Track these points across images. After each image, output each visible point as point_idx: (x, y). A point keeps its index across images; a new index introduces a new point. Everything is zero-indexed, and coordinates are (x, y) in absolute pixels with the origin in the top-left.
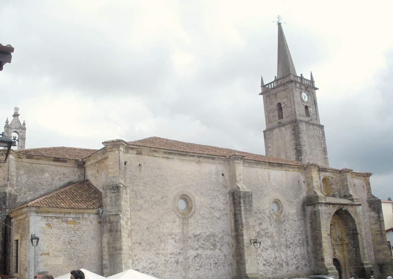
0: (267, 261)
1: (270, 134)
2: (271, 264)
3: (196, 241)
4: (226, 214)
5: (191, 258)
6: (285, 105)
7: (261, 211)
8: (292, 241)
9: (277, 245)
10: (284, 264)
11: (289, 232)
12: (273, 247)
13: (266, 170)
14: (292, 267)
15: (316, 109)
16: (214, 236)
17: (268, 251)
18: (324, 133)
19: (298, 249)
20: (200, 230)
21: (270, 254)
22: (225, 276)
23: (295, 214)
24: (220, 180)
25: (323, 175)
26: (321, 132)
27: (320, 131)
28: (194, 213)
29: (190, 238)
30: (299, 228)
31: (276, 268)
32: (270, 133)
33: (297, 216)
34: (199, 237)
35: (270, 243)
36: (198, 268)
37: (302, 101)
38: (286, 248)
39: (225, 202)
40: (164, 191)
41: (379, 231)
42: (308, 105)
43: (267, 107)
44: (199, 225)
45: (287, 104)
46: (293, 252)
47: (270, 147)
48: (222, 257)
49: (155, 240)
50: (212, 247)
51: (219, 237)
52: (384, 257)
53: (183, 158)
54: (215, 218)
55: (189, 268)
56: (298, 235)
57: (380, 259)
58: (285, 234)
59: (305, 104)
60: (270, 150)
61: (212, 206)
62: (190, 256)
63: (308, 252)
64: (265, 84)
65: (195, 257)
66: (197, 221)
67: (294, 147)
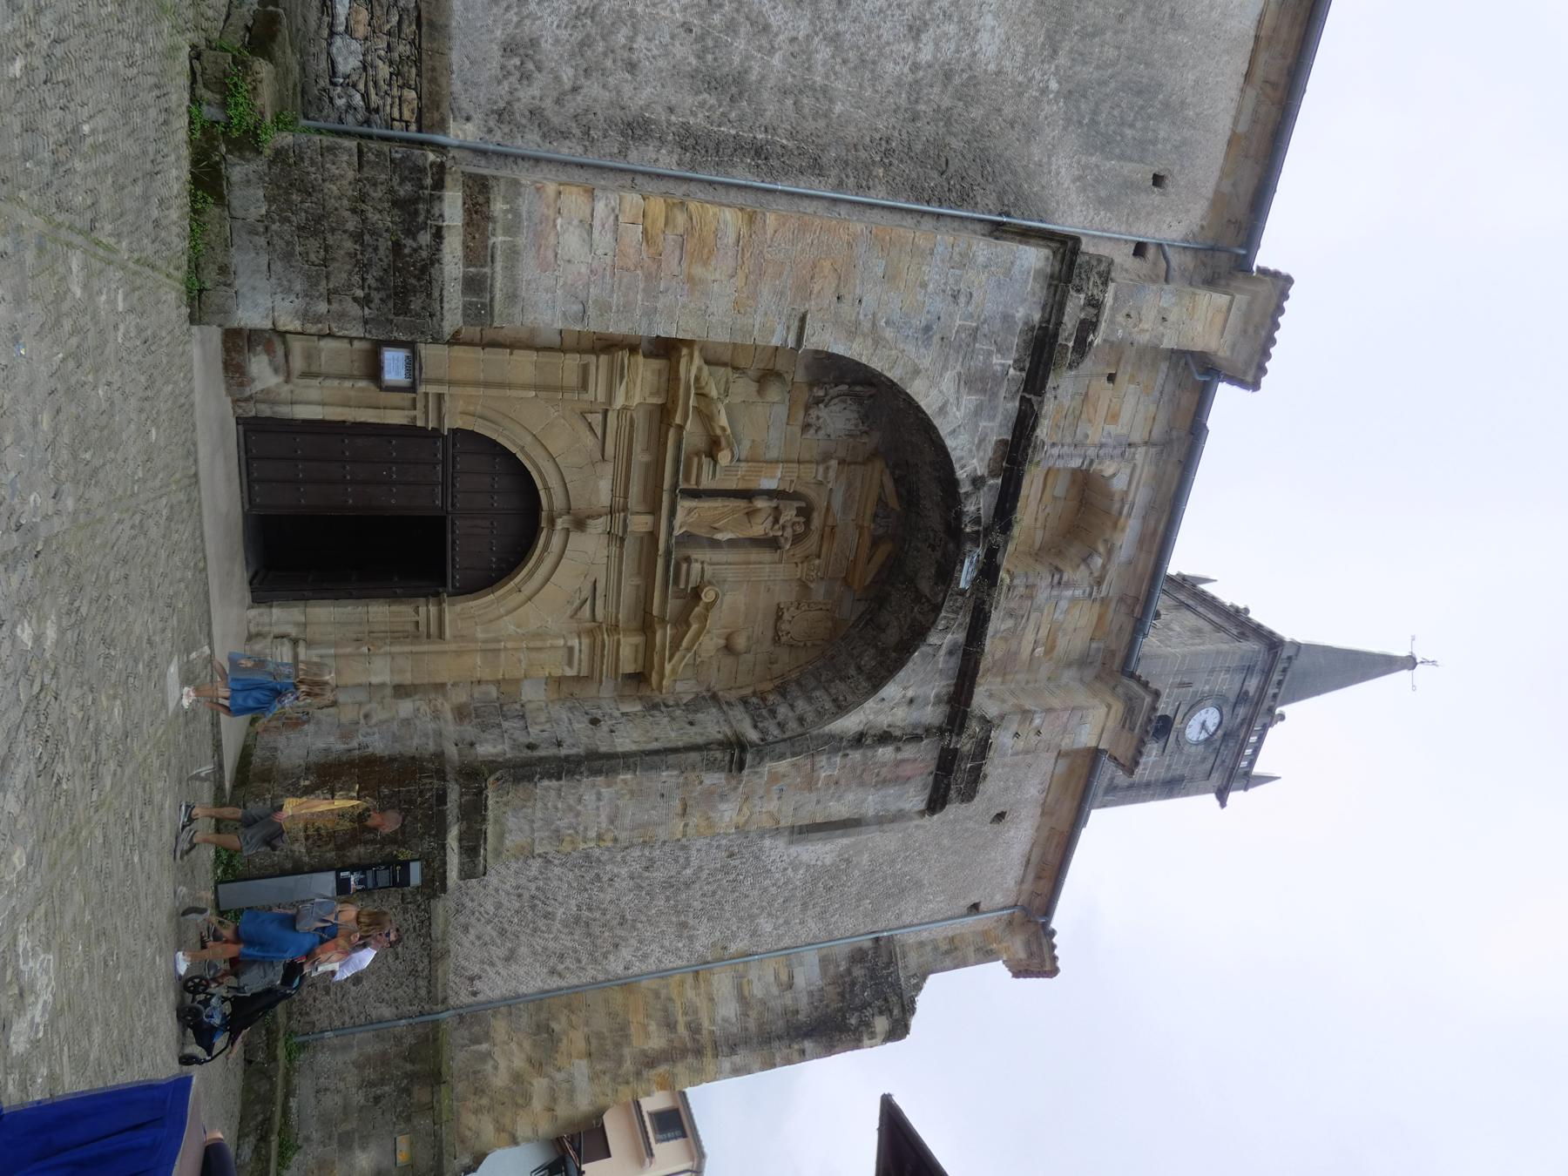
37: (1195, 706)
41: (695, 1029)
52: (500, 1080)
57: (484, 1047)
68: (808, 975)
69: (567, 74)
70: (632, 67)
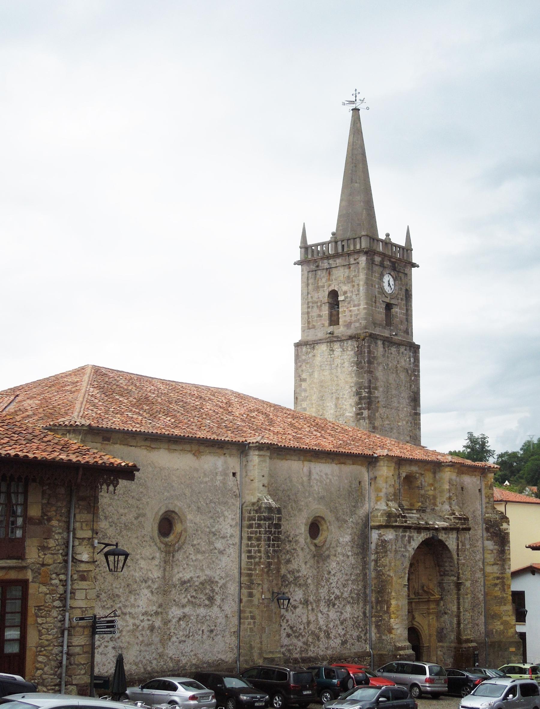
0: (294, 629)
1: (307, 353)
2: (301, 634)
3: (183, 592)
4: (233, 544)
5: (174, 621)
6: (346, 298)
7: (290, 539)
8: (339, 594)
9: (312, 601)
10: (322, 635)
11: (335, 576)
12: (306, 603)
13: (306, 463)
14: (335, 640)
15: (407, 310)
16: (213, 582)
17: (297, 610)
18: (419, 362)
19: (348, 608)
20: (191, 571)
21: (299, 617)
22: (223, 653)
23: (349, 543)
24: (230, 483)
25: (404, 471)
26: (412, 360)
27: (409, 358)
28: (184, 543)
29: (175, 586)
30: (352, 570)
31: (308, 641)
32: (309, 350)
33: (353, 547)
34: (189, 584)
35: (301, 596)
36: (183, 638)
38: (328, 606)
39: (234, 523)
40: (141, 506)
41: (498, 578)
42: (393, 302)
43: (308, 293)
44: (190, 563)
45: (351, 297)
46: (338, 614)
47: (304, 380)
48: (221, 620)
49: (121, 590)
50: (207, 602)
51: (219, 585)
52: (502, 627)
53: (173, 447)
54: (216, 551)
55: (170, 639)
56: (350, 582)
57: (494, 630)
58: (328, 580)
59: (388, 300)
60: (304, 385)
61: (214, 530)
62: (172, 617)
63: (364, 613)
64: (310, 242)
65: (180, 619)
66: (187, 557)
67: (354, 389)
68: (490, 545)
69: (360, 630)
70: (358, 617)
